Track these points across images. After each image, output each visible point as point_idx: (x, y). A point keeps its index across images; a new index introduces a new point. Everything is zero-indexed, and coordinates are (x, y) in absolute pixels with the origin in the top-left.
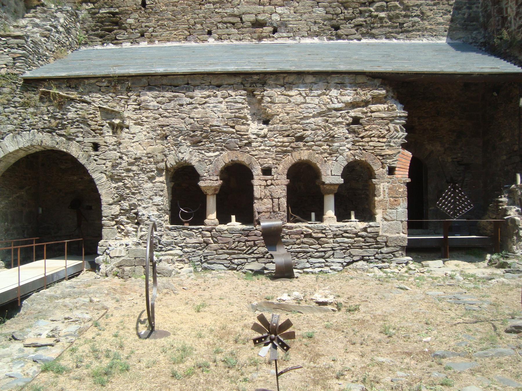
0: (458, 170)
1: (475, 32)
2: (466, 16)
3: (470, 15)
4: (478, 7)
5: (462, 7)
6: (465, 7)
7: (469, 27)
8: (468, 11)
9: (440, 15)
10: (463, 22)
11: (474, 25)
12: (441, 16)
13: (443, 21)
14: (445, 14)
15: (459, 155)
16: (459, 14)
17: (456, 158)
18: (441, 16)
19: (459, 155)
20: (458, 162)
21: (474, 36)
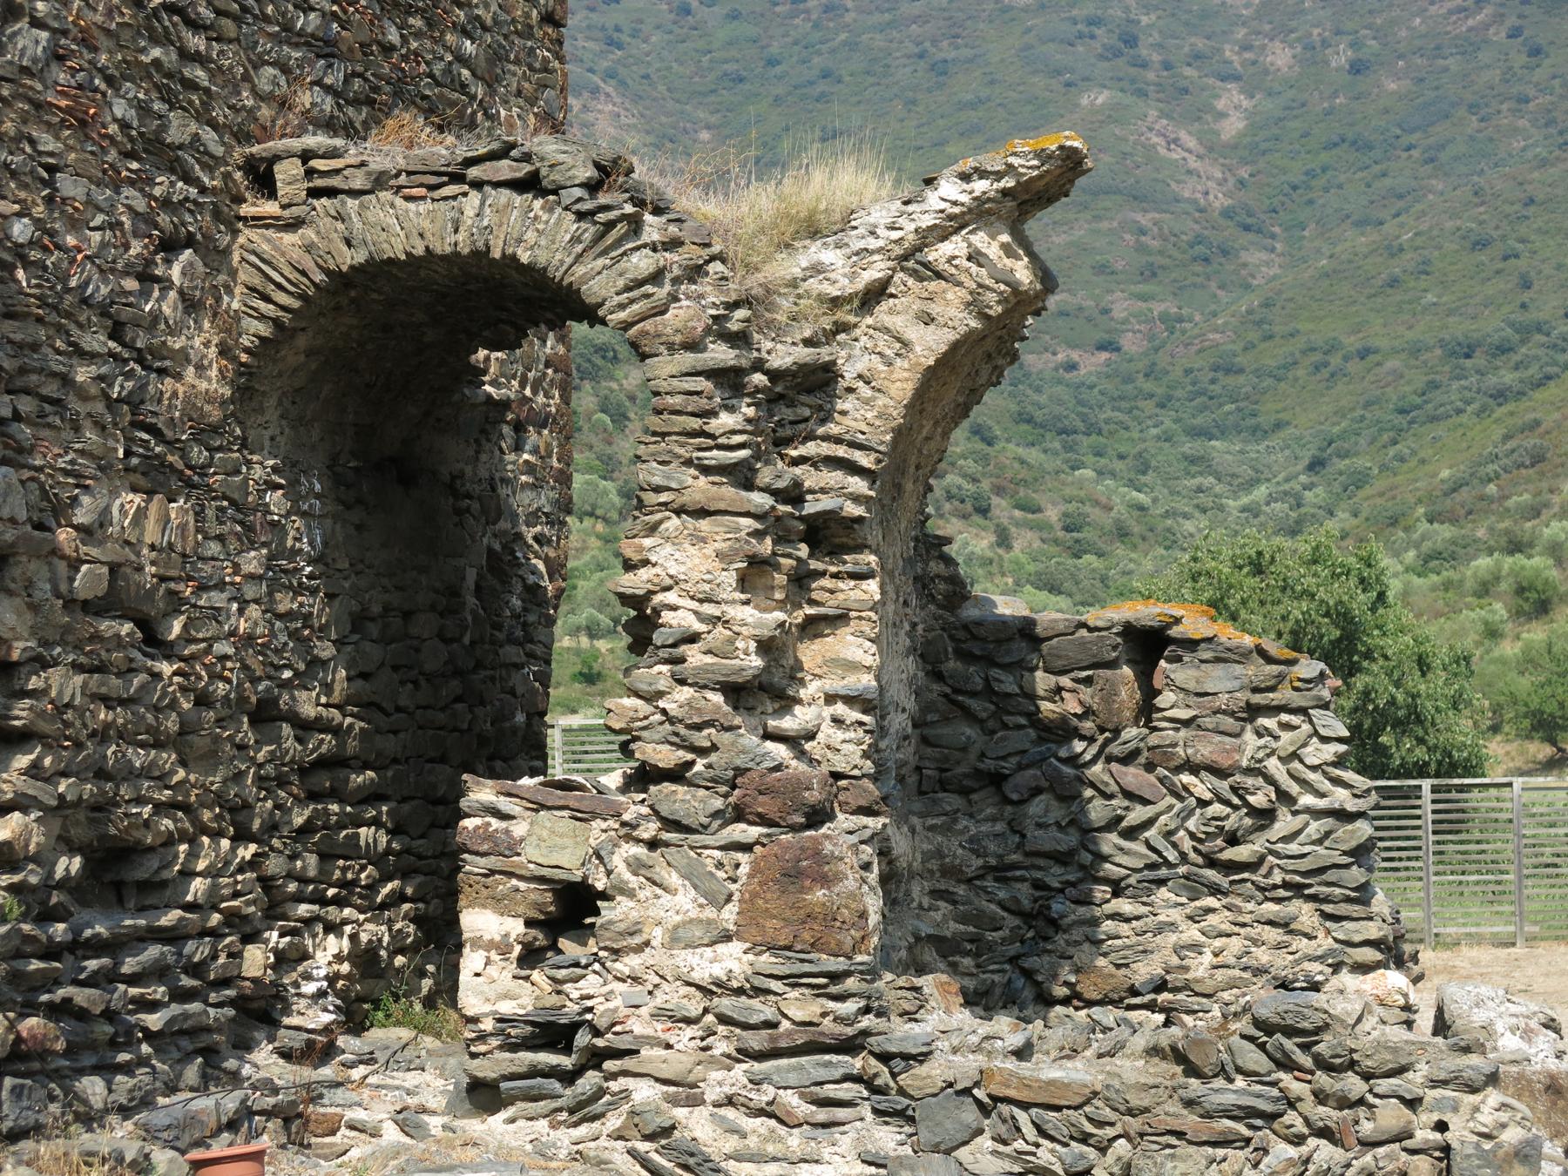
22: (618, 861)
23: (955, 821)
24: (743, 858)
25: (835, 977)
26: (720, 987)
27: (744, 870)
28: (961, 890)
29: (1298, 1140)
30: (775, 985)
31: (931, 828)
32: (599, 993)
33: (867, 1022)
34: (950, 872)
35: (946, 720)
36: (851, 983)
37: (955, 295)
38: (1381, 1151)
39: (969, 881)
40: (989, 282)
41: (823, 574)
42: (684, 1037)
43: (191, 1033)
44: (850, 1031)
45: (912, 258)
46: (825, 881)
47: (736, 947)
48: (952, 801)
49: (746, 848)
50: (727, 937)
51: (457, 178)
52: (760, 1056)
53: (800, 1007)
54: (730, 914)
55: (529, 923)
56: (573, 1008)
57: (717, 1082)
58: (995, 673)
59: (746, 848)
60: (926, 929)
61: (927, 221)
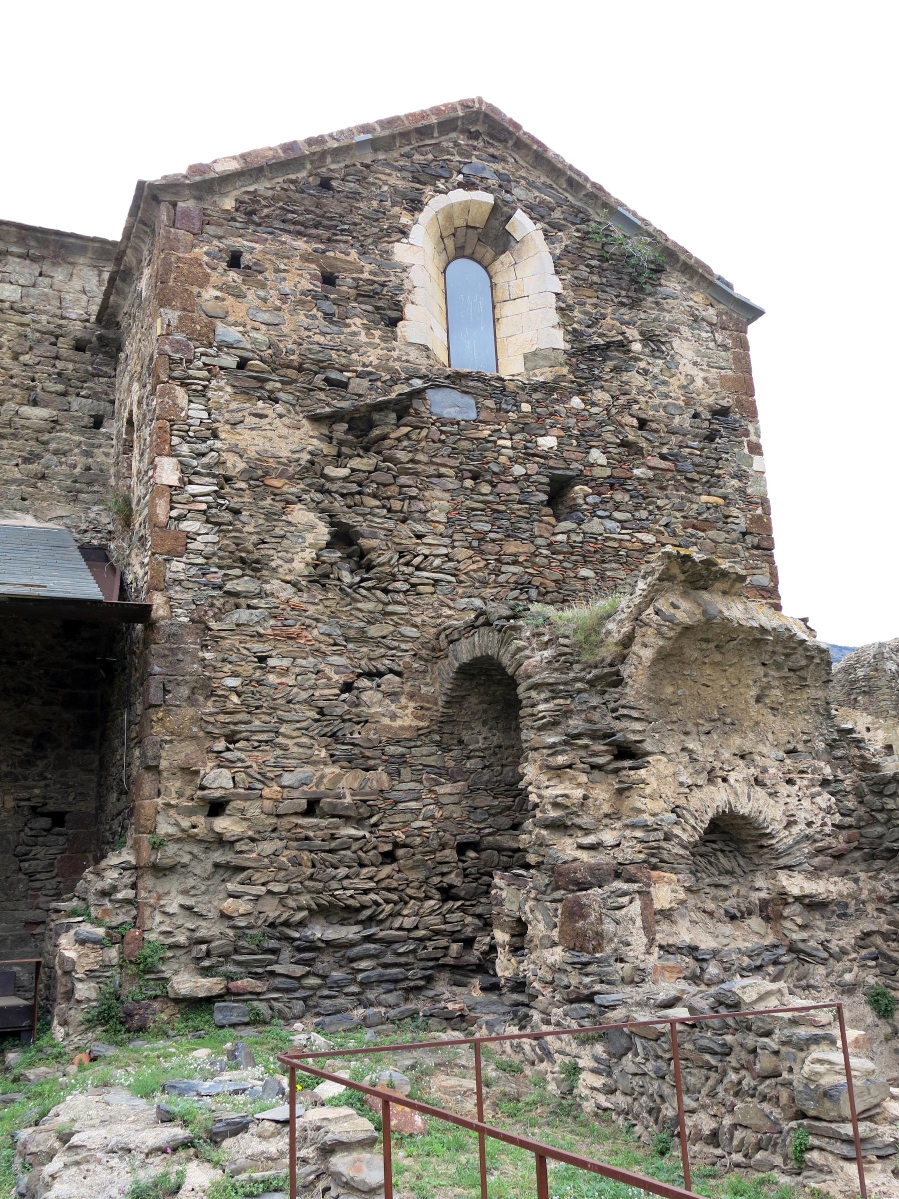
0: (31, 829)
1: (95, 508)
2: (78, 470)
3: (88, 469)
4: (107, 455)
5: (71, 450)
6: (76, 451)
7: (82, 496)
8: (83, 459)
9: (15, 462)
10: (69, 482)
11: (96, 492)
12: (17, 465)
13: (19, 476)
14: (26, 461)
15: (37, 791)
16: (61, 463)
17: (29, 800)
18: (17, 465)
19: (37, 791)
20: (33, 809)
21: (92, 515)
22: (527, 908)
23: (878, 874)
24: (559, 906)
25: (586, 964)
26: (554, 969)
27: (559, 912)
28: (888, 908)
29: (736, 1070)
30: (569, 968)
31: (870, 878)
32: (528, 968)
33: (597, 987)
34: (880, 899)
35: (869, 825)
36: (590, 969)
37: (650, 631)
38: (768, 1082)
39: (891, 903)
40: (662, 622)
41: (625, 768)
42: (548, 991)
43: (396, 981)
44: (586, 992)
45: (637, 619)
46: (584, 917)
47: (559, 950)
48: (878, 864)
49: (560, 901)
50: (554, 944)
51: (474, 627)
52: (571, 1002)
53: (573, 979)
54: (555, 934)
55: (513, 936)
56: (521, 975)
57: (557, 1013)
58: (886, 800)
59: (560, 901)
60: (873, 928)
61: (637, 601)
